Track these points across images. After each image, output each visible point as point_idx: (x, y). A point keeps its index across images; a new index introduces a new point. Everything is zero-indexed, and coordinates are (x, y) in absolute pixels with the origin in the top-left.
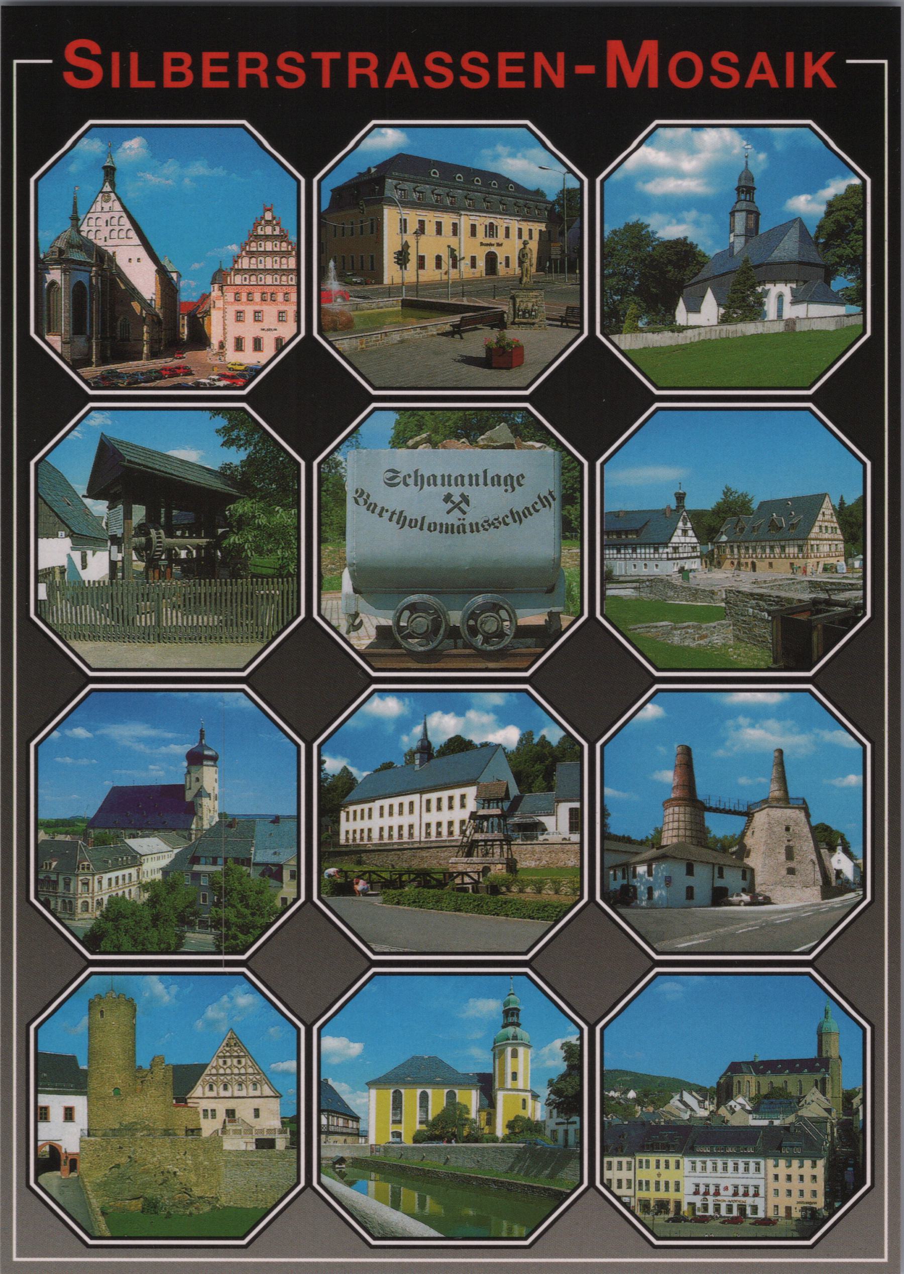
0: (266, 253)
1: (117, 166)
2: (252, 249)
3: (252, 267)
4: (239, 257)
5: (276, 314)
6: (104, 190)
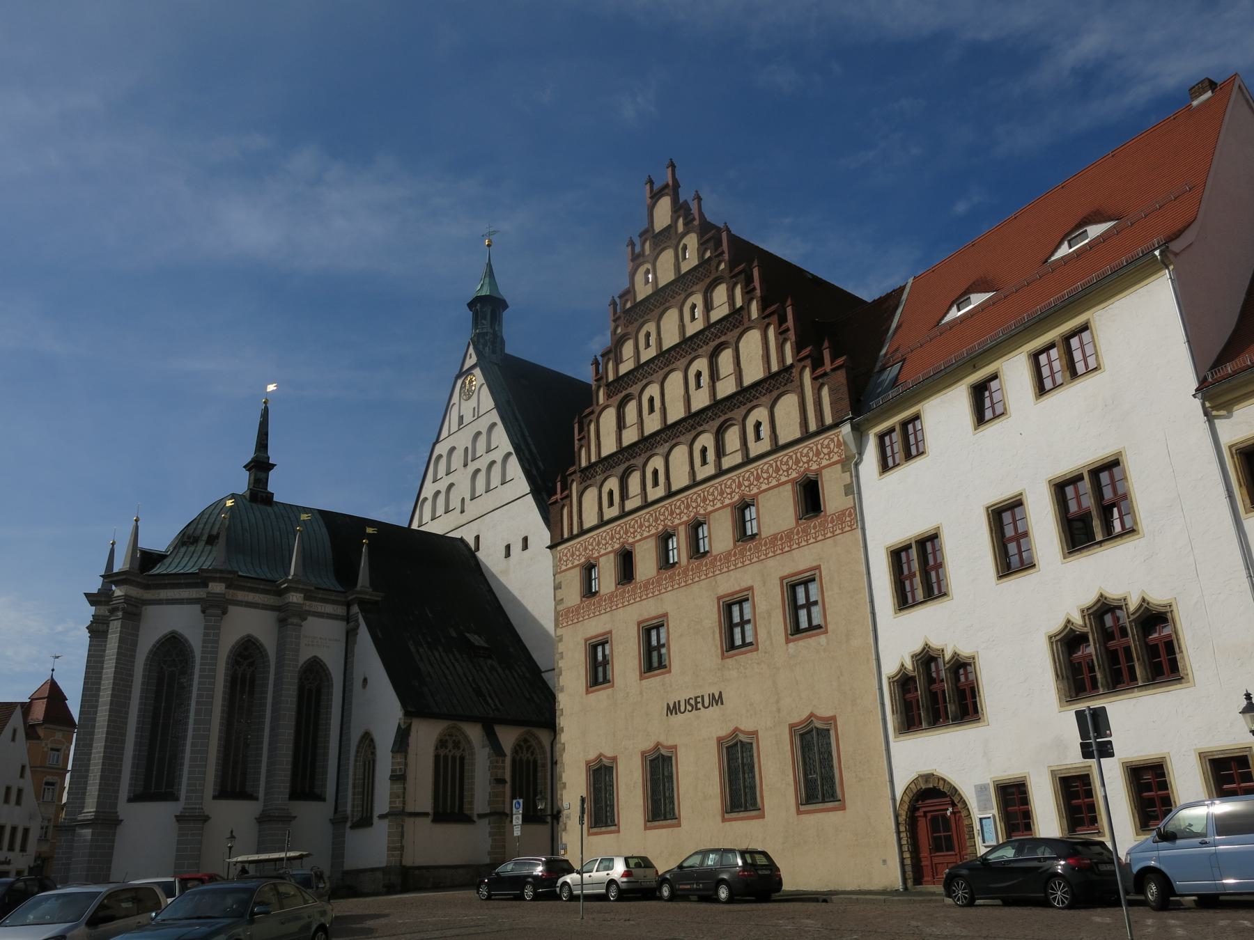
0: (666, 359)
1: (505, 292)
2: (624, 368)
5: (711, 617)
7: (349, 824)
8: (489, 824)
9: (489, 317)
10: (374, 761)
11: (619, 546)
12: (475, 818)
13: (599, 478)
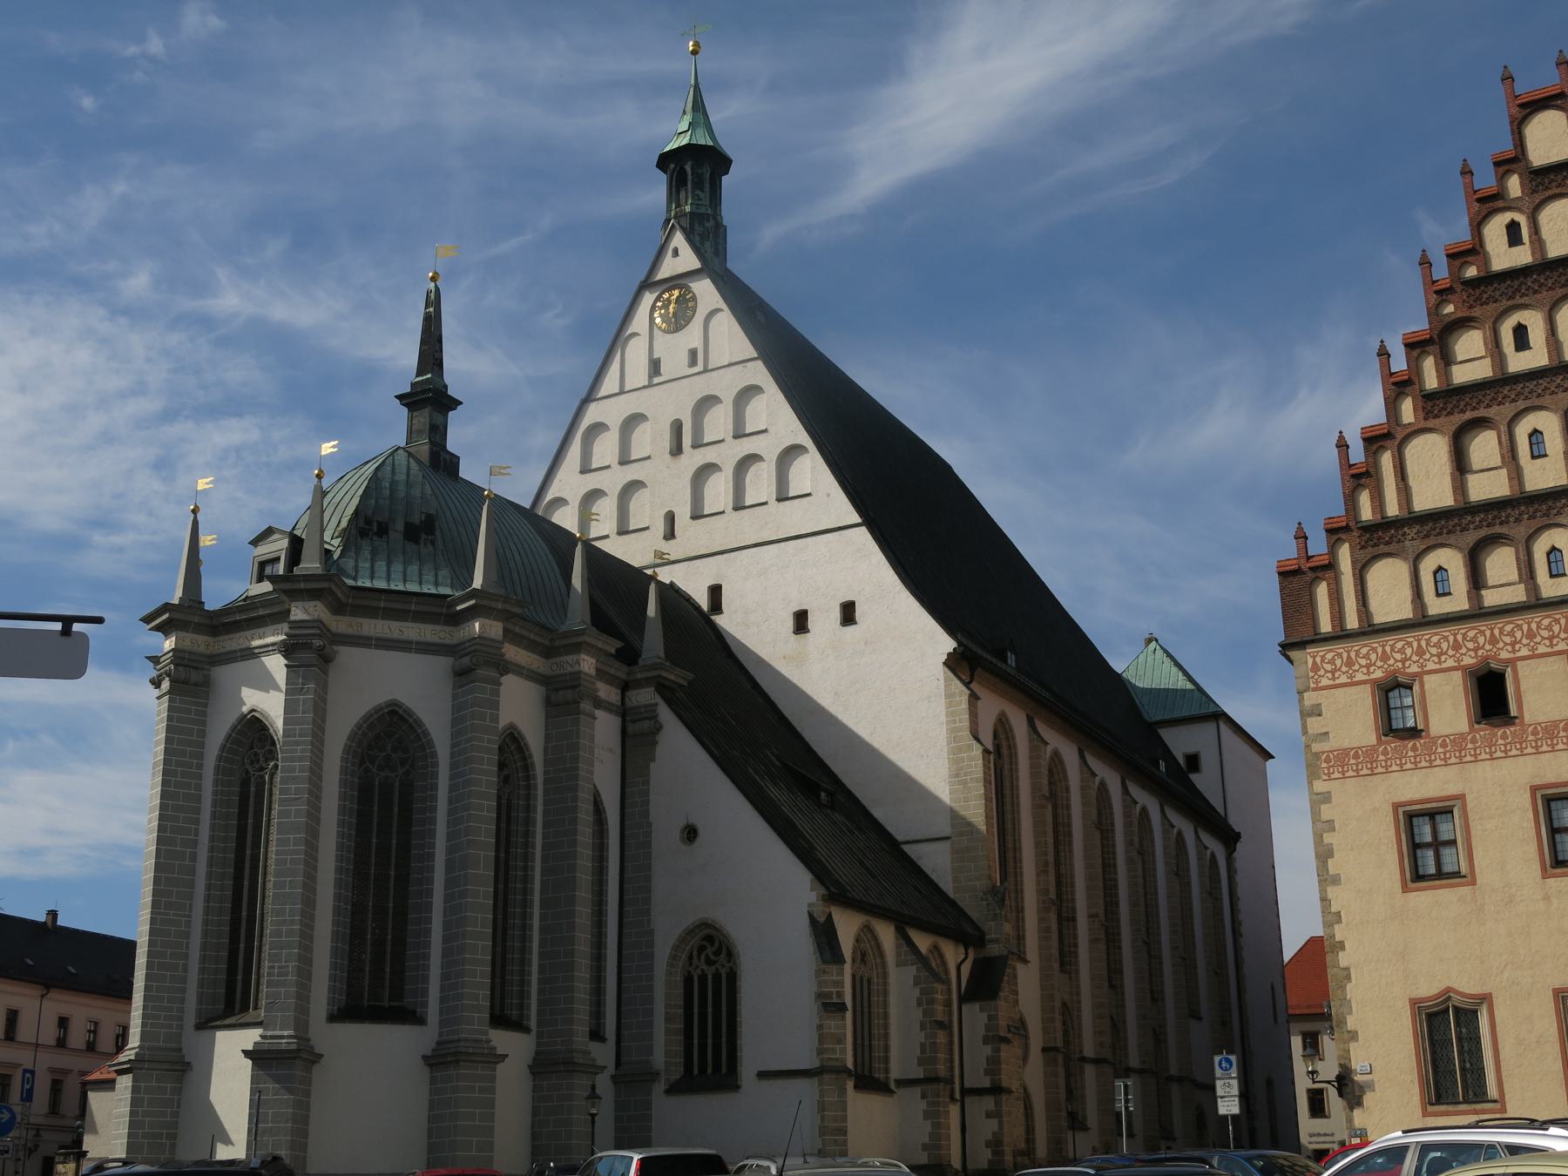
2: (1462, 375)
3: (1488, 486)
4: (1375, 440)
6: (669, 268)
7: (659, 1087)
8: (923, 1097)
9: (707, 185)
10: (733, 977)
11: (1474, 661)
12: (893, 1086)
13: (1411, 546)
